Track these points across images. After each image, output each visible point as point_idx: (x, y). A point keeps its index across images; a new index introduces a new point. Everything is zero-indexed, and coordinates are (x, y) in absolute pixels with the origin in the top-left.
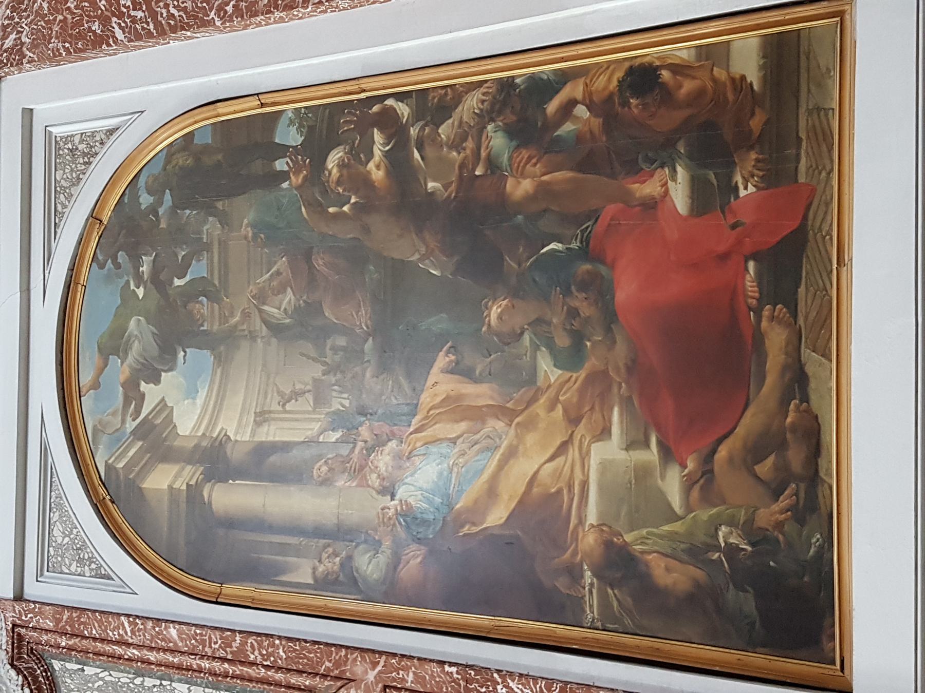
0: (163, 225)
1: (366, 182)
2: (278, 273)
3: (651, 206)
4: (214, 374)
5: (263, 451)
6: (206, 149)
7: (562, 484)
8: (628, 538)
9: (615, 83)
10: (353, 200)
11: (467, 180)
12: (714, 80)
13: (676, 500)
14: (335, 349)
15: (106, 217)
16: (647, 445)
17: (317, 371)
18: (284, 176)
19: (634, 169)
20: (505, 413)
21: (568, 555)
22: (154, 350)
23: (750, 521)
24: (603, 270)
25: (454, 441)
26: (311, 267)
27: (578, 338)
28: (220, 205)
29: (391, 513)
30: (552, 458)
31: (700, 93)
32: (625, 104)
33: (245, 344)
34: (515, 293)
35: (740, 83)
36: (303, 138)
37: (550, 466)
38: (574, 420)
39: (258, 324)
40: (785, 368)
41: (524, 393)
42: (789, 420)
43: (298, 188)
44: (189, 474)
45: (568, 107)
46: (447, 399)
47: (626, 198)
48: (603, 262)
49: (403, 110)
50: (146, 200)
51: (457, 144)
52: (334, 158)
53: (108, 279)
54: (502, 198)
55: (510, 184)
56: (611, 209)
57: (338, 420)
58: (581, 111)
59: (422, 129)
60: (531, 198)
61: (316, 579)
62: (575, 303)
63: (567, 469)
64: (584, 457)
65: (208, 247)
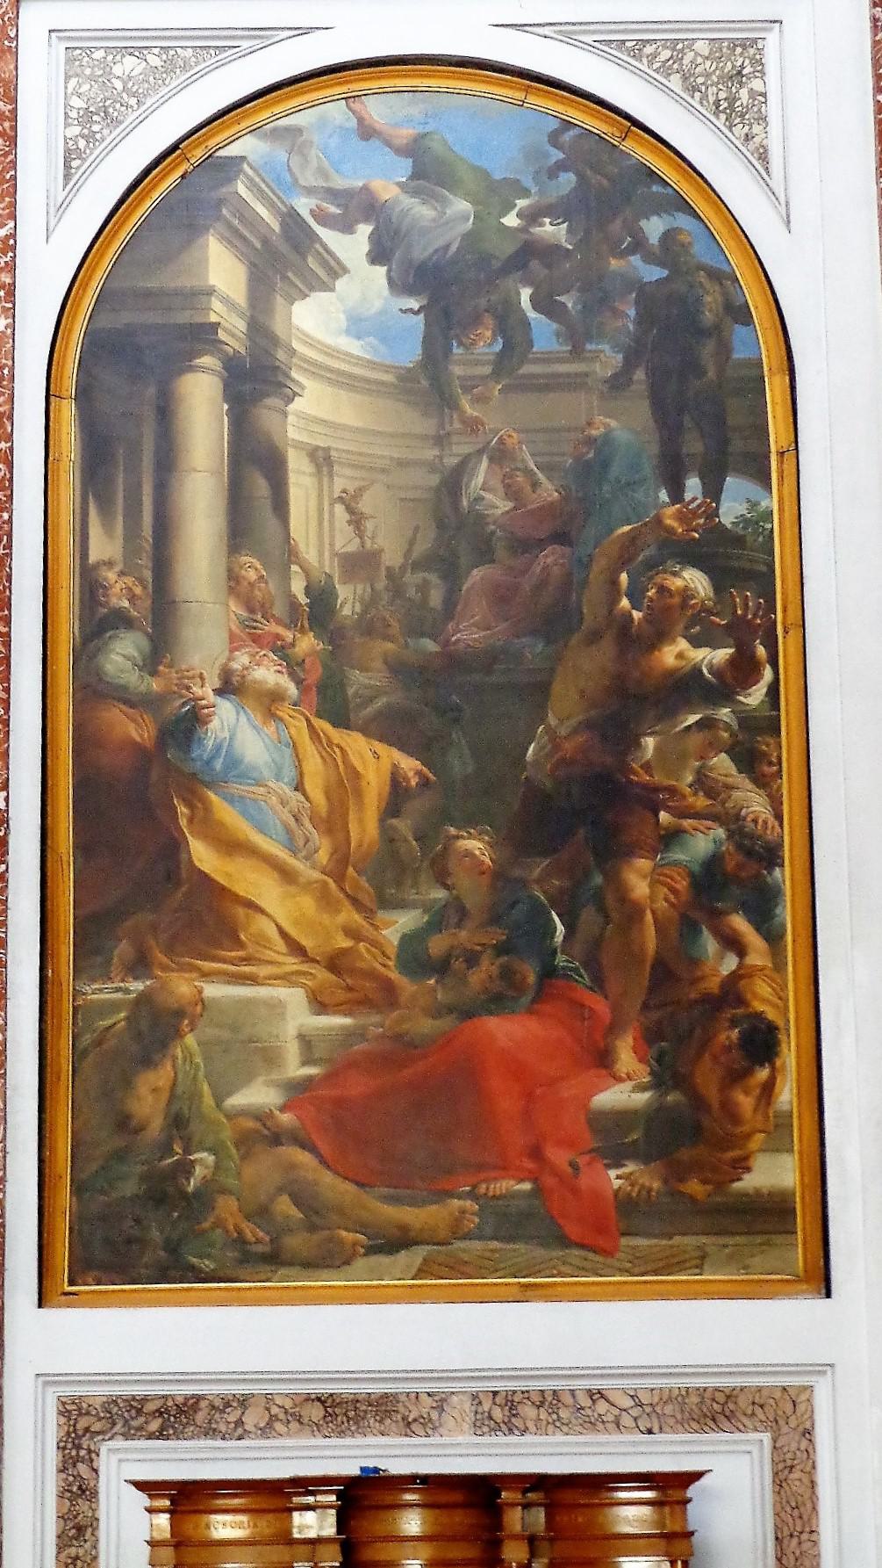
0: (615, 264)
1: (660, 636)
2: (535, 485)
3: (603, 1060)
4: (387, 369)
5: (275, 468)
6: (724, 349)
7: (251, 949)
8: (190, 1040)
9: (759, 1007)
10: (636, 615)
11: (651, 800)
12: (748, 1136)
13: (238, 1100)
14: (424, 588)
15: (628, 146)
16: (304, 1063)
17: (392, 556)
18: (677, 495)
19: (650, 1037)
20: (337, 870)
21: (165, 960)
22: (422, 251)
23: (224, 1191)
24: (525, 1000)
25: (299, 787)
26: (541, 544)
27: (441, 968)
28: (640, 375)
29: (197, 690)
30: (283, 934)
31: (733, 1116)
32: (734, 1023)
33: (427, 426)
34: (499, 876)
35: (742, 1165)
36: (729, 526)
37: (272, 932)
38: (335, 963)
39: (461, 448)
40: (404, 1228)
41: (367, 897)
42: (344, 1233)
43: (658, 520)
44: (232, 326)
45: (734, 944)
46: (356, 775)
47: (614, 1029)
48: (533, 1001)
49: (755, 697)
50: (654, 227)
51: (703, 783)
52: (695, 580)
53: (533, 154)
54: (630, 852)
55: (643, 864)
56: (600, 1005)
57: (321, 602)
58: (730, 963)
59: (728, 727)
60: (623, 897)
61: (97, 566)
62: (485, 963)
63: (270, 955)
64: (287, 979)
65: (577, 352)
